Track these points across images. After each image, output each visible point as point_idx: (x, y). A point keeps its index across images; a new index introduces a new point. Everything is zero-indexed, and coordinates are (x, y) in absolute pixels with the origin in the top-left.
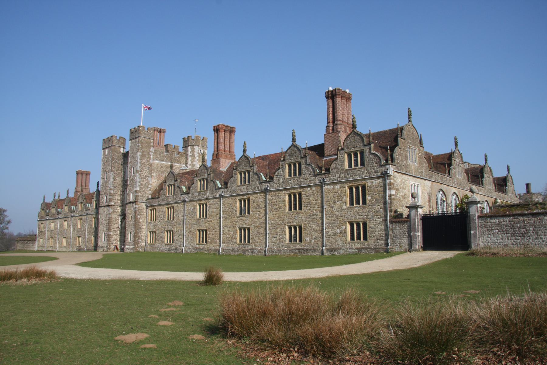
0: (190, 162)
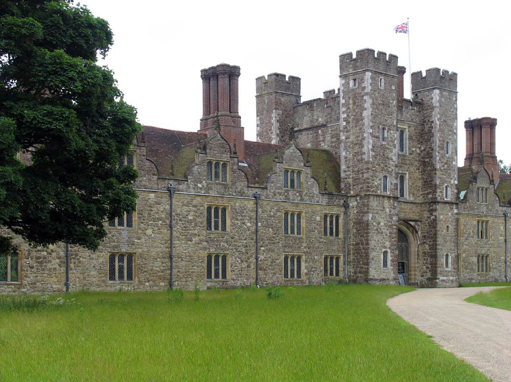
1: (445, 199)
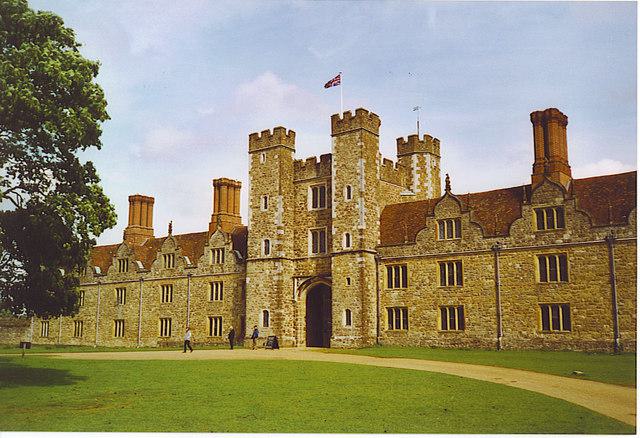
0: (416, 182)
1: (345, 248)
